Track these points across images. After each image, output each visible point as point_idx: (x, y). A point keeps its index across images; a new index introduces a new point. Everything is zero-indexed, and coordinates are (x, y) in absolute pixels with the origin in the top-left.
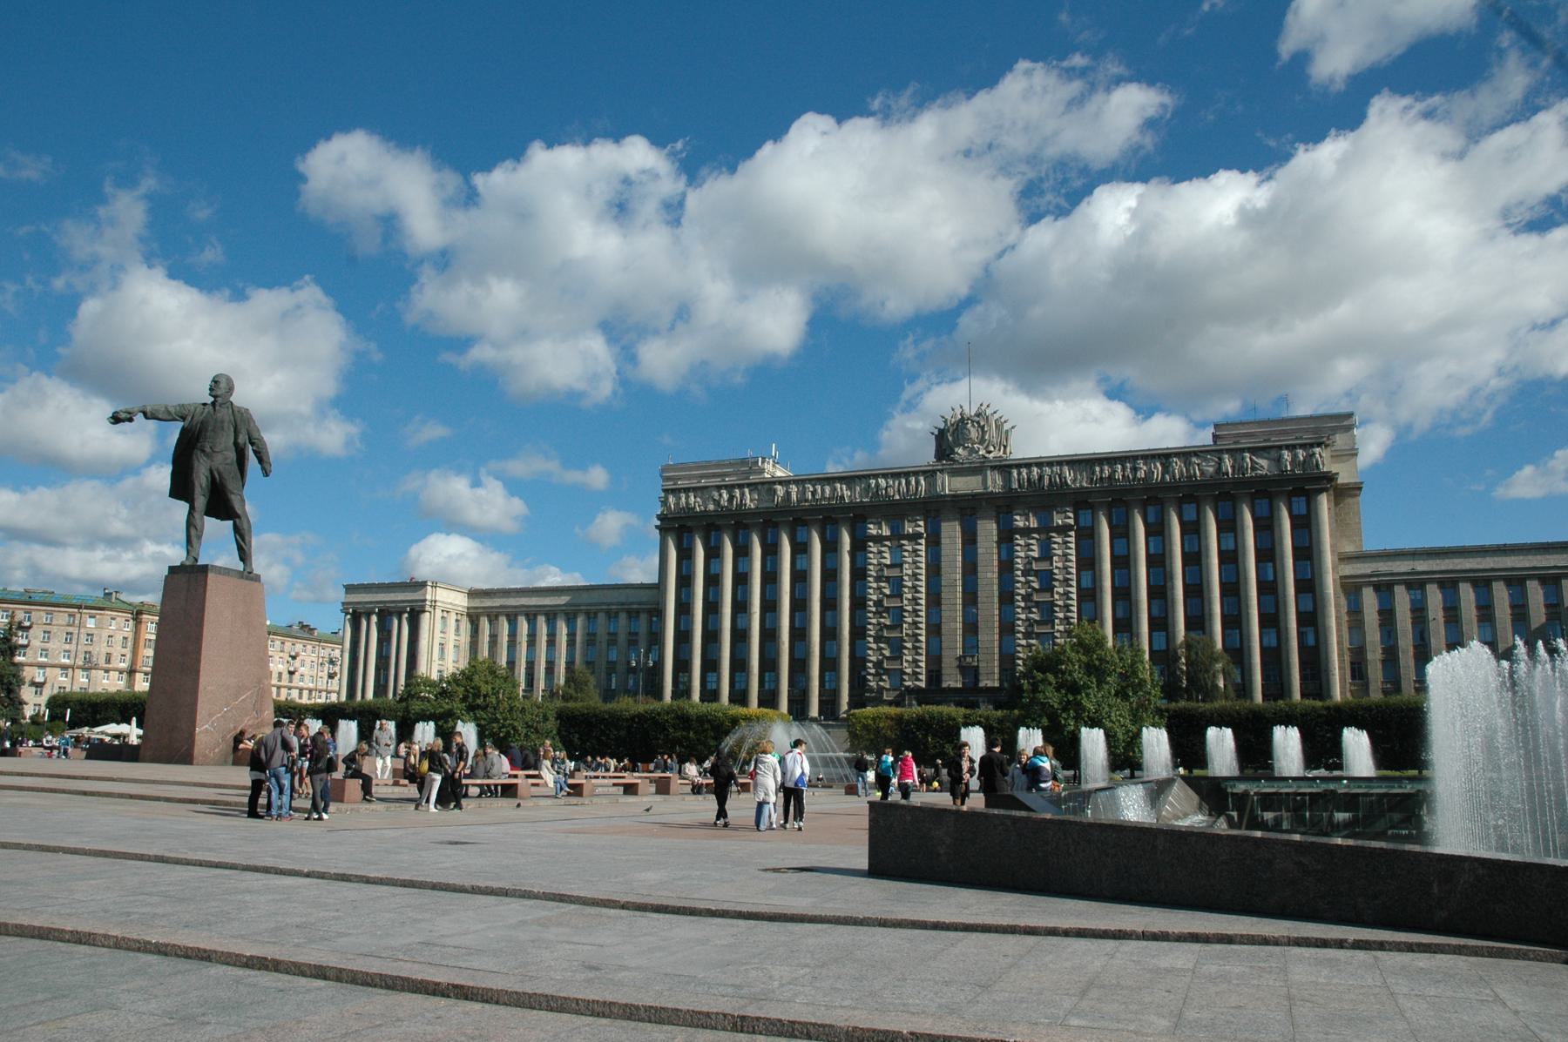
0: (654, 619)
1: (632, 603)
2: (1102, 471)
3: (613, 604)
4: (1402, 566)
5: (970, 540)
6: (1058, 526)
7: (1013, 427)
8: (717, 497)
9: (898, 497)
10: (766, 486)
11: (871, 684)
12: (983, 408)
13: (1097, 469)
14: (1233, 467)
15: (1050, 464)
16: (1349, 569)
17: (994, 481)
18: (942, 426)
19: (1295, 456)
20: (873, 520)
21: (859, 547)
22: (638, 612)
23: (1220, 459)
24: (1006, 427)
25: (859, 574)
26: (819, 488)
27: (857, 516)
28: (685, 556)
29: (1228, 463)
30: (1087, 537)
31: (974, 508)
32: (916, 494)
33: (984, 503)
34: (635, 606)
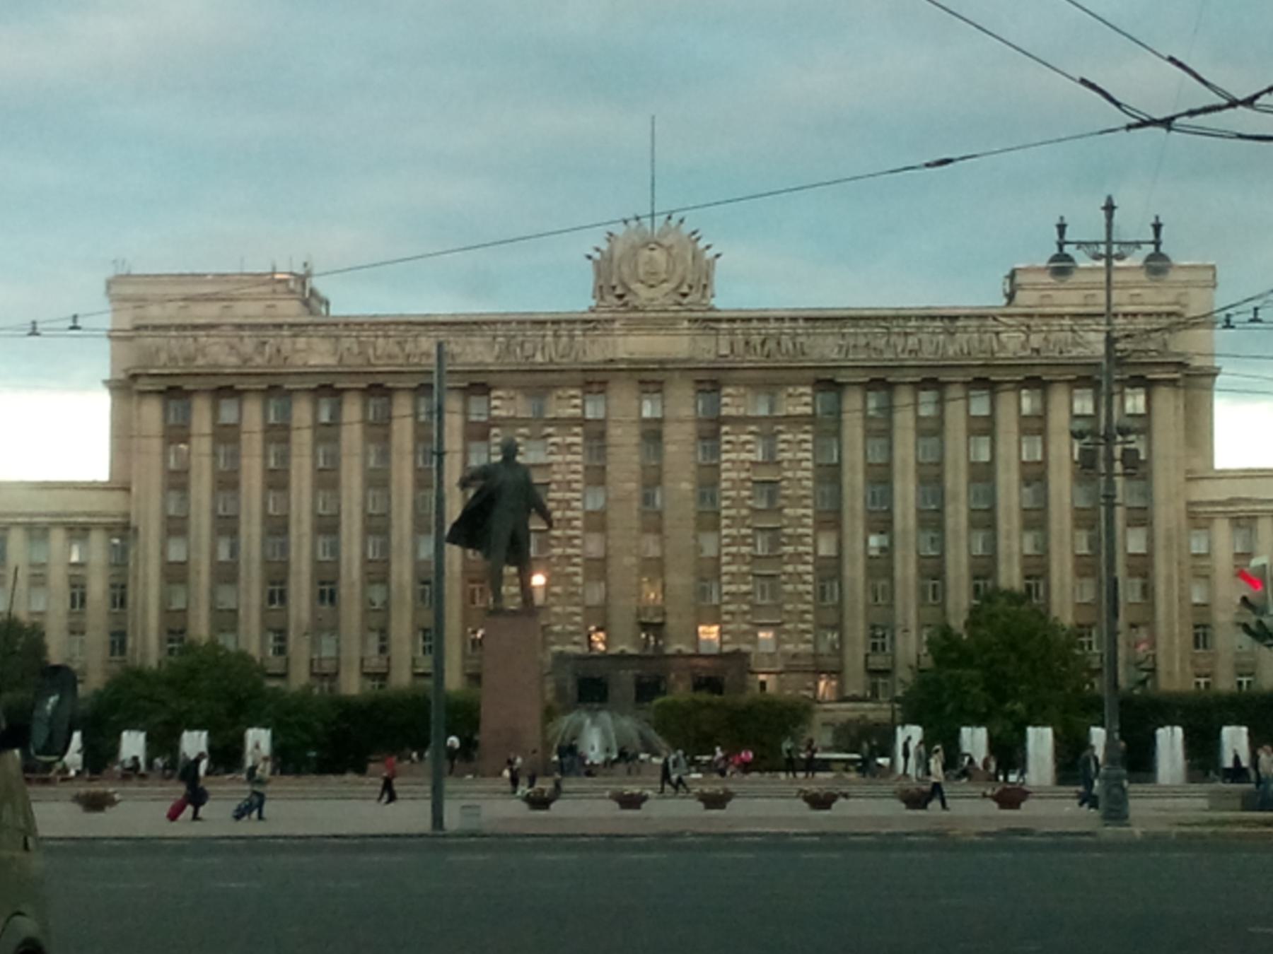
3: (39, 515)
7: (718, 256)
9: (539, 358)
18: (604, 247)
20: (500, 393)
23: (1028, 327)
28: (177, 434)
31: (661, 383)
32: (569, 355)
34: (81, 520)
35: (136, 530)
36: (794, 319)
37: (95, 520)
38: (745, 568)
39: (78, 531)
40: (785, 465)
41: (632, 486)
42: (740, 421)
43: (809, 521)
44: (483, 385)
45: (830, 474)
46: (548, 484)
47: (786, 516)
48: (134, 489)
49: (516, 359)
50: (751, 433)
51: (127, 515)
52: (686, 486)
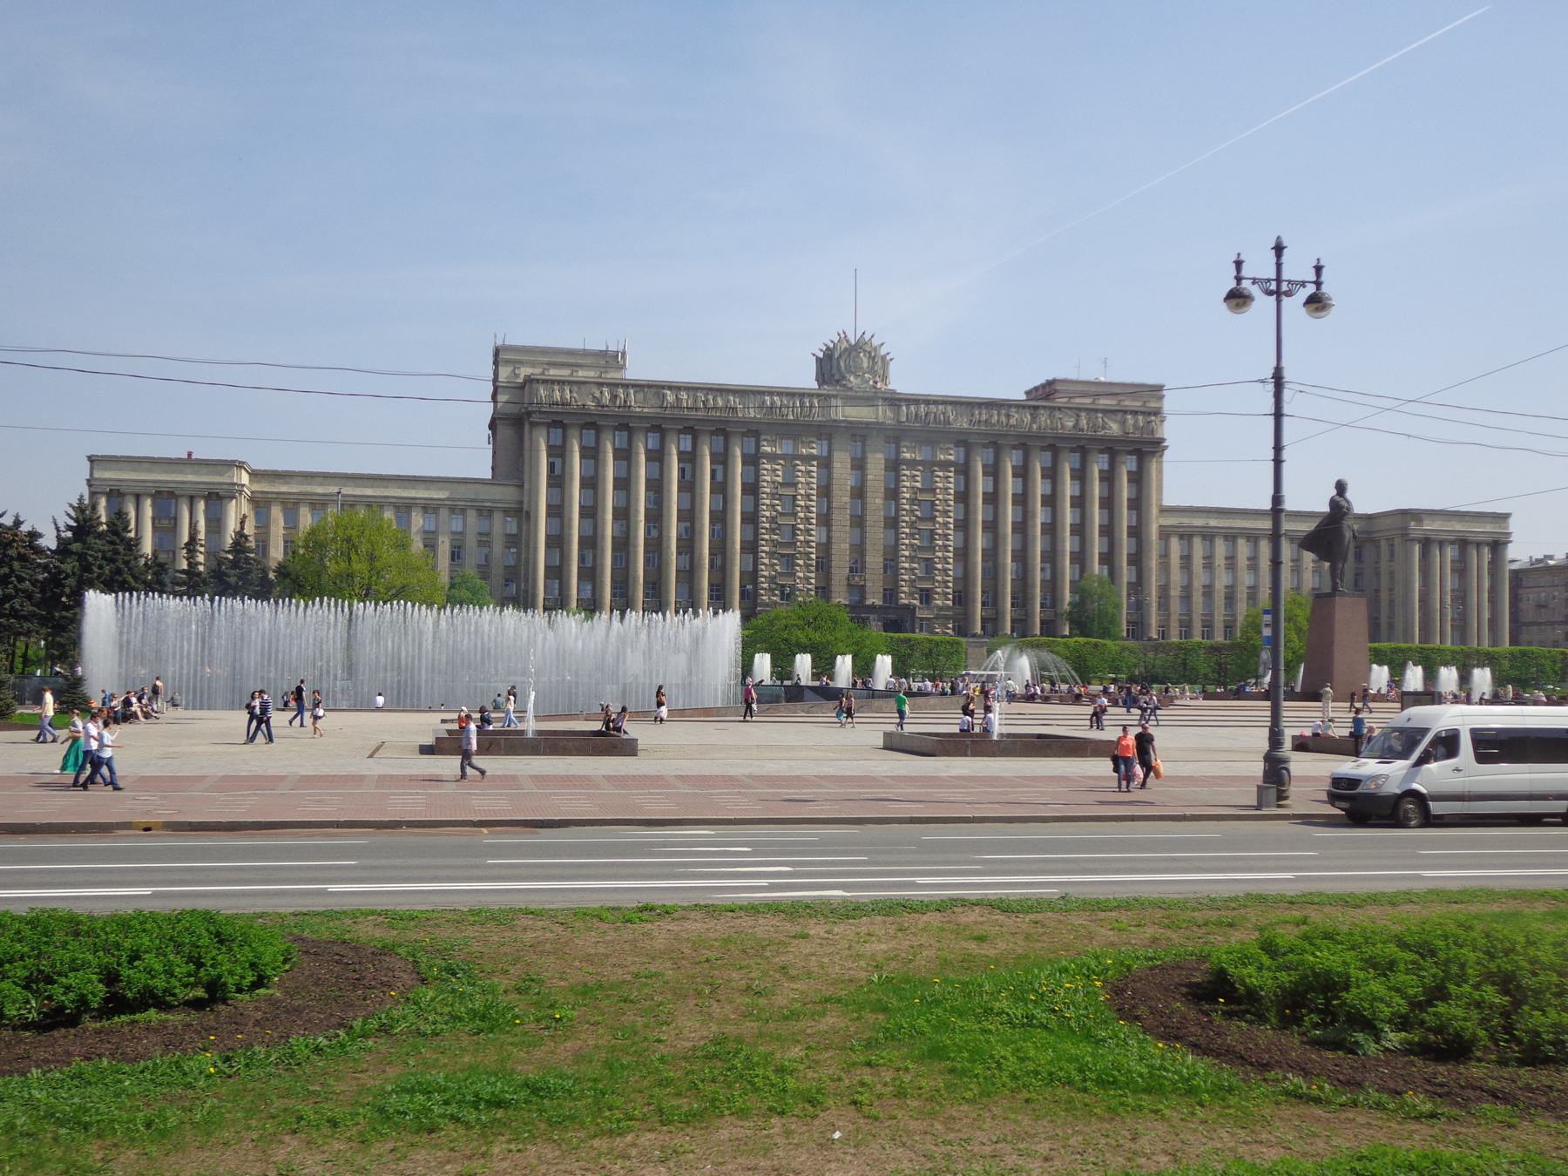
0: (509, 519)
1: (483, 501)
2: (980, 414)
3: (459, 500)
4: (1199, 522)
5: (859, 465)
6: (941, 461)
8: (597, 394)
10: (653, 390)
11: (764, 598)
12: (867, 337)
13: (977, 412)
14: (1088, 424)
15: (936, 403)
16: (1171, 521)
17: (884, 412)
19: (1136, 421)
20: (769, 438)
21: (752, 461)
22: (490, 511)
23: (1078, 416)
24: (888, 358)
25: (752, 489)
26: (711, 397)
27: (754, 431)
29: (1084, 422)
30: (964, 470)
33: (875, 432)
34: (489, 504)
35: (528, 514)
36: (944, 403)
37: (499, 505)
38: (913, 554)
39: (485, 512)
40: (938, 491)
41: (848, 499)
42: (912, 464)
43: (952, 526)
44: (757, 431)
45: (964, 497)
46: (794, 497)
47: (939, 523)
48: (526, 486)
49: (776, 417)
50: (919, 470)
51: (521, 502)
52: (879, 501)
